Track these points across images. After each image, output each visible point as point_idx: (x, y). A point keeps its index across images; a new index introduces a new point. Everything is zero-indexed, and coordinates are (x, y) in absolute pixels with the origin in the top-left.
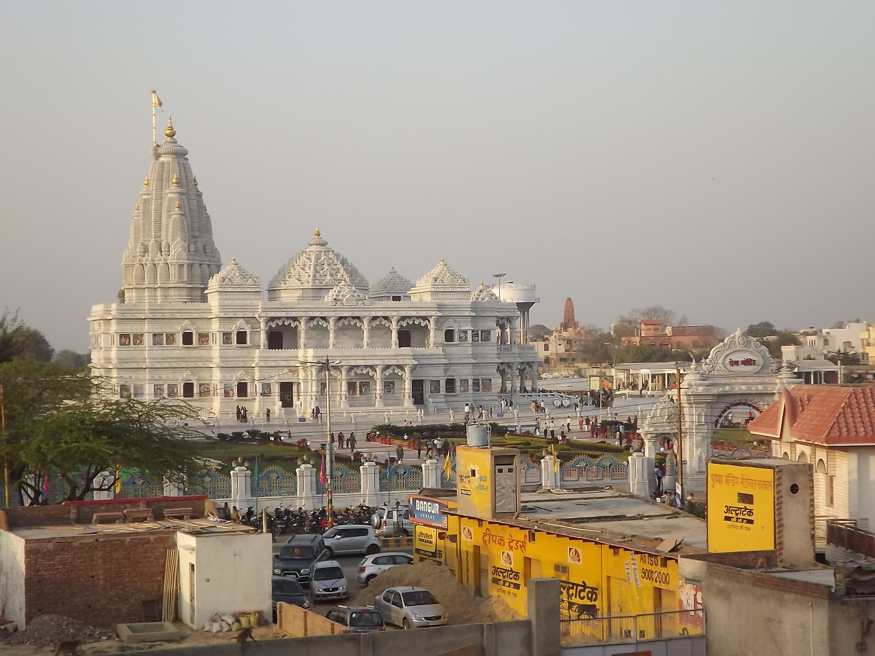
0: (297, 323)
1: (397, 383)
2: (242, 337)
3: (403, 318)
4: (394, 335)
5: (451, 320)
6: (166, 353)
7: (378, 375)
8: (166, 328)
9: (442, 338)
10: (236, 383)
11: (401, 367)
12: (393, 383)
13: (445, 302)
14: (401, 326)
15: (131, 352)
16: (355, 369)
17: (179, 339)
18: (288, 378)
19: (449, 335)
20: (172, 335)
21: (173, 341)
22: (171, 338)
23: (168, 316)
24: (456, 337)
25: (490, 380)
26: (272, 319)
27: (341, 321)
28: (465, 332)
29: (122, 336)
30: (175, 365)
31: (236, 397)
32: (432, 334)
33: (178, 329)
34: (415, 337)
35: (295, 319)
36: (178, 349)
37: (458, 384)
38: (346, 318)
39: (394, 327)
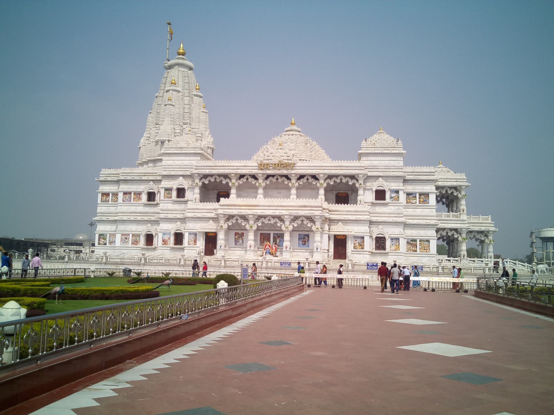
0: (228, 180)
1: (311, 234)
3: (330, 177)
4: (322, 192)
5: (380, 179)
6: (133, 209)
7: (287, 227)
9: (370, 197)
10: (173, 232)
11: (311, 219)
12: (308, 236)
13: (375, 163)
16: (262, 220)
17: (144, 197)
18: (210, 227)
19: (380, 195)
20: (140, 194)
21: (140, 199)
23: (137, 178)
24: (388, 195)
26: (206, 176)
28: (397, 192)
30: (139, 218)
32: (360, 192)
33: (144, 188)
34: (351, 197)
35: (226, 176)
37: (388, 243)
38: (273, 176)
39: (322, 183)
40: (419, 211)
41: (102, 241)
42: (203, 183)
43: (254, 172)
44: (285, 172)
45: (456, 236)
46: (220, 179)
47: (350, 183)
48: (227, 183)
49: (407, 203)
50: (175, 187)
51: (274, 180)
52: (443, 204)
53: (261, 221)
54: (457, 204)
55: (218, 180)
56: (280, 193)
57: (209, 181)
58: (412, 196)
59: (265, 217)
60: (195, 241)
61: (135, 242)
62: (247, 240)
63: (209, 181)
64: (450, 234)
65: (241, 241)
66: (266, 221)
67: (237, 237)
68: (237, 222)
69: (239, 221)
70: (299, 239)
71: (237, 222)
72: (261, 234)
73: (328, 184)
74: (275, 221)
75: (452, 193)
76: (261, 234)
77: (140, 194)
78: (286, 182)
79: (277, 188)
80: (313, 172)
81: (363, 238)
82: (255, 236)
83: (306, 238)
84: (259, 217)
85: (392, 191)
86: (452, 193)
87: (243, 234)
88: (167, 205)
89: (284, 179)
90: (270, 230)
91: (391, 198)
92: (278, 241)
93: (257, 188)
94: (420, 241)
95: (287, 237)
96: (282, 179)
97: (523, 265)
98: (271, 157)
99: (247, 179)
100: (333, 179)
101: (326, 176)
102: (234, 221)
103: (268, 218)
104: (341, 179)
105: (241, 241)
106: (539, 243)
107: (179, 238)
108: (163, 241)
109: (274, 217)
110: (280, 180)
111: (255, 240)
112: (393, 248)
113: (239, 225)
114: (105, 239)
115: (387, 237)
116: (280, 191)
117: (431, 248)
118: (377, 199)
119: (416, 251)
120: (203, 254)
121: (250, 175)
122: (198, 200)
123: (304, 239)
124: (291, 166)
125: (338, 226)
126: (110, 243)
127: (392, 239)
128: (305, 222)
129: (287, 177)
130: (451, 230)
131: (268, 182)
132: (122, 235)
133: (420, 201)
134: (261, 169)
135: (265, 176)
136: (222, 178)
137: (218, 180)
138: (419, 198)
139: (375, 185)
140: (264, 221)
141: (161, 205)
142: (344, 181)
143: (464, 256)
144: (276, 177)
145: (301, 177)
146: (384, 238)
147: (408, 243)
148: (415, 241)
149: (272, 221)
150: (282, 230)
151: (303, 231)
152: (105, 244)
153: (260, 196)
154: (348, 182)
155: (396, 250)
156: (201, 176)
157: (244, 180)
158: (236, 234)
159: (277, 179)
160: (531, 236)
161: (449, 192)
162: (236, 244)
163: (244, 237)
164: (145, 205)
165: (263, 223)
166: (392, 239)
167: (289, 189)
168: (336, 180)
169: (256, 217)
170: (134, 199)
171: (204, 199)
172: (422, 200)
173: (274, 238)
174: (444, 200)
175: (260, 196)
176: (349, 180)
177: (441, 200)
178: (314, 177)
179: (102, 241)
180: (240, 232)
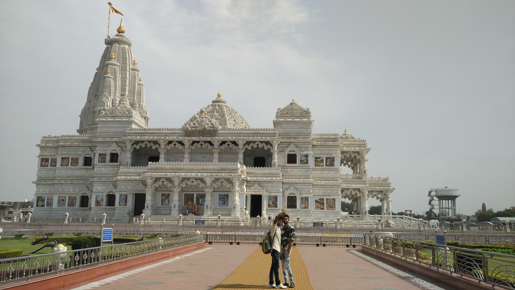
2: (114, 158)
3: (248, 143)
4: (241, 156)
6: (70, 172)
8: (71, 154)
10: (105, 195)
12: (227, 196)
14: (246, 149)
15: (48, 172)
17: (81, 161)
18: (139, 188)
19: (292, 159)
22: (75, 162)
25: (334, 200)
26: (137, 142)
27: (195, 145)
28: (307, 156)
29: (42, 160)
31: (104, 207)
35: (155, 142)
36: (79, 171)
38: (198, 142)
40: (325, 174)
41: (40, 203)
42: (135, 149)
43: (180, 138)
44: (209, 139)
45: (358, 195)
46: (150, 145)
47: (266, 148)
48: (157, 149)
49: (315, 166)
50: (108, 153)
51: (199, 145)
52: (349, 166)
53: (185, 182)
54: (360, 167)
55: (148, 146)
56: (205, 157)
57: (140, 146)
58: (320, 159)
59: (188, 179)
60: (126, 202)
61: (72, 204)
62: (172, 201)
63: (140, 146)
64: (353, 193)
65: (167, 201)
66: (190, 183)
67: (163, 198)
68: (163, 184)
69: (165, 183)
70: (219, 199)
71: (163, 184)
72: (185, 195)
73: (246, 149)
74: (197, 182)
75: (355, 157)
76: (185, 195)
77: (77, 159)
78: (210, 147)
79: (201, 153)
80: (234, 138)
81: (276, 197)
82: (180, 196)
83: (226, 197)
84: (184, 179)
85: (302, 155)
86: (355, 157)
87: (169, 194)
88: (101, 169)
89: (208, 144)
90: (193, 191)
91: (301, 161)
92: (200, 201)
93: (184, 153)
94: (327, 199)
95: (208, 198)
96: (206, 145)
97: (394, 217)
98: (197, 125)
99: (175, 145)
100: (251, 145)
101: (245, 142)
102: (160, 183)
103: (191, 180)
104: (258, 145)
105: (167, 201)
106: (436, 202)
107: (111, 200)
108: (96, 202)
109: (197, 179)
110: (204, 146)
111: (179, 200)
112: (303, 206)
113: (166, 187)
114: (43, 201)
115: (298, 197)
116: (205, 155)
117: (336, 206)
118: (289, 162)
119: (323, 209)
120: (132, 214)
121: (177, 141)
122: (129, 163)
123: (225, 199)
124: (213, 132)
125: (254, 187)
126: (48, 205)
127: (302, 199)
128: (224, 184)
129: (210, 143)
130: (354, 189)
131: (193, 147)
132: (59, 197)
133: (326, 164)
134: (187, 136)
135: (191, 142)
136: (152, 144)
137: (148, 146)
138: (326, 162)
139: (287, 152)
140: (188, 182)
141: (96, 169)
142: (260, 146)
143: (366, 213)
144: (200, 143)
145: (223, 143)
146: (295, 197)
147: (316, 201)
148: (323, 199)
149: (195, 183)
150: (204, 191)
151: (223, 191)
152: (43, 206)
153: (186, 160)
154: (264, 147)
155: (305, 208)
156: (133, 142)
157: (172, 145)
158: (163, 195)
159: (202, 145)
160: (429, 195)
161: (353, 156)
162: (162, 204)
163: (170, 198)
164: (81, 169)
165: (187, 184)
166: (302, 199)
167: (212, 153)
168: (253, 145)
169: (181, 179)
170: (71, 163)
171: (134, 164)
172: (328, 163)
173: (197, 198)
174: (349, 163)
175: (186, 160)
176: (265, 145)
177: (347, 163)
178: (234, 143)
179: (40, 203)
180: (166, 193)
